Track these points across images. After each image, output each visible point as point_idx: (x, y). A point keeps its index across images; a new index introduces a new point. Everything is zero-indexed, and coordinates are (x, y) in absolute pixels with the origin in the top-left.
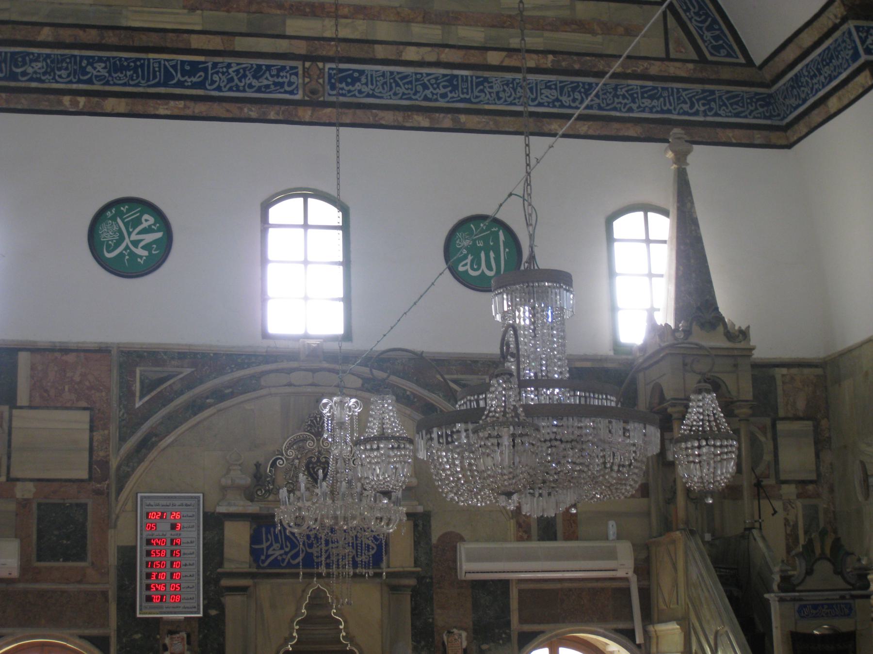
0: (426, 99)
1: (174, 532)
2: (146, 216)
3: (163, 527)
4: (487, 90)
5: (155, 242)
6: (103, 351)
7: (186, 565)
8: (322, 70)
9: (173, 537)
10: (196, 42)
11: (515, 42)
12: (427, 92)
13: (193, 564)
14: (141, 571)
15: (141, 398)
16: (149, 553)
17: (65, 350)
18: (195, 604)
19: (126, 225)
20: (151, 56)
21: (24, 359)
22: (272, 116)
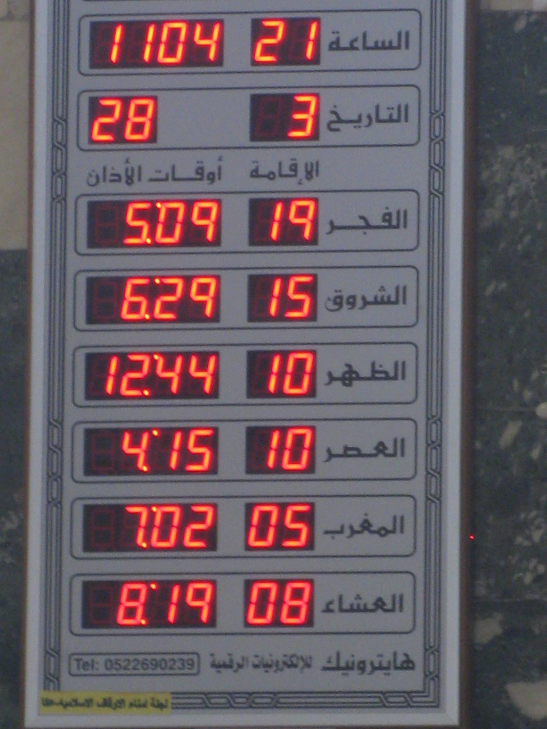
1: (271, 156)
3: (202, 118)
7: (350, 377)
9: (263, 188)
13: (398, 372)
14: (54, 423)
16: (104, 298)
18: (413, 646)
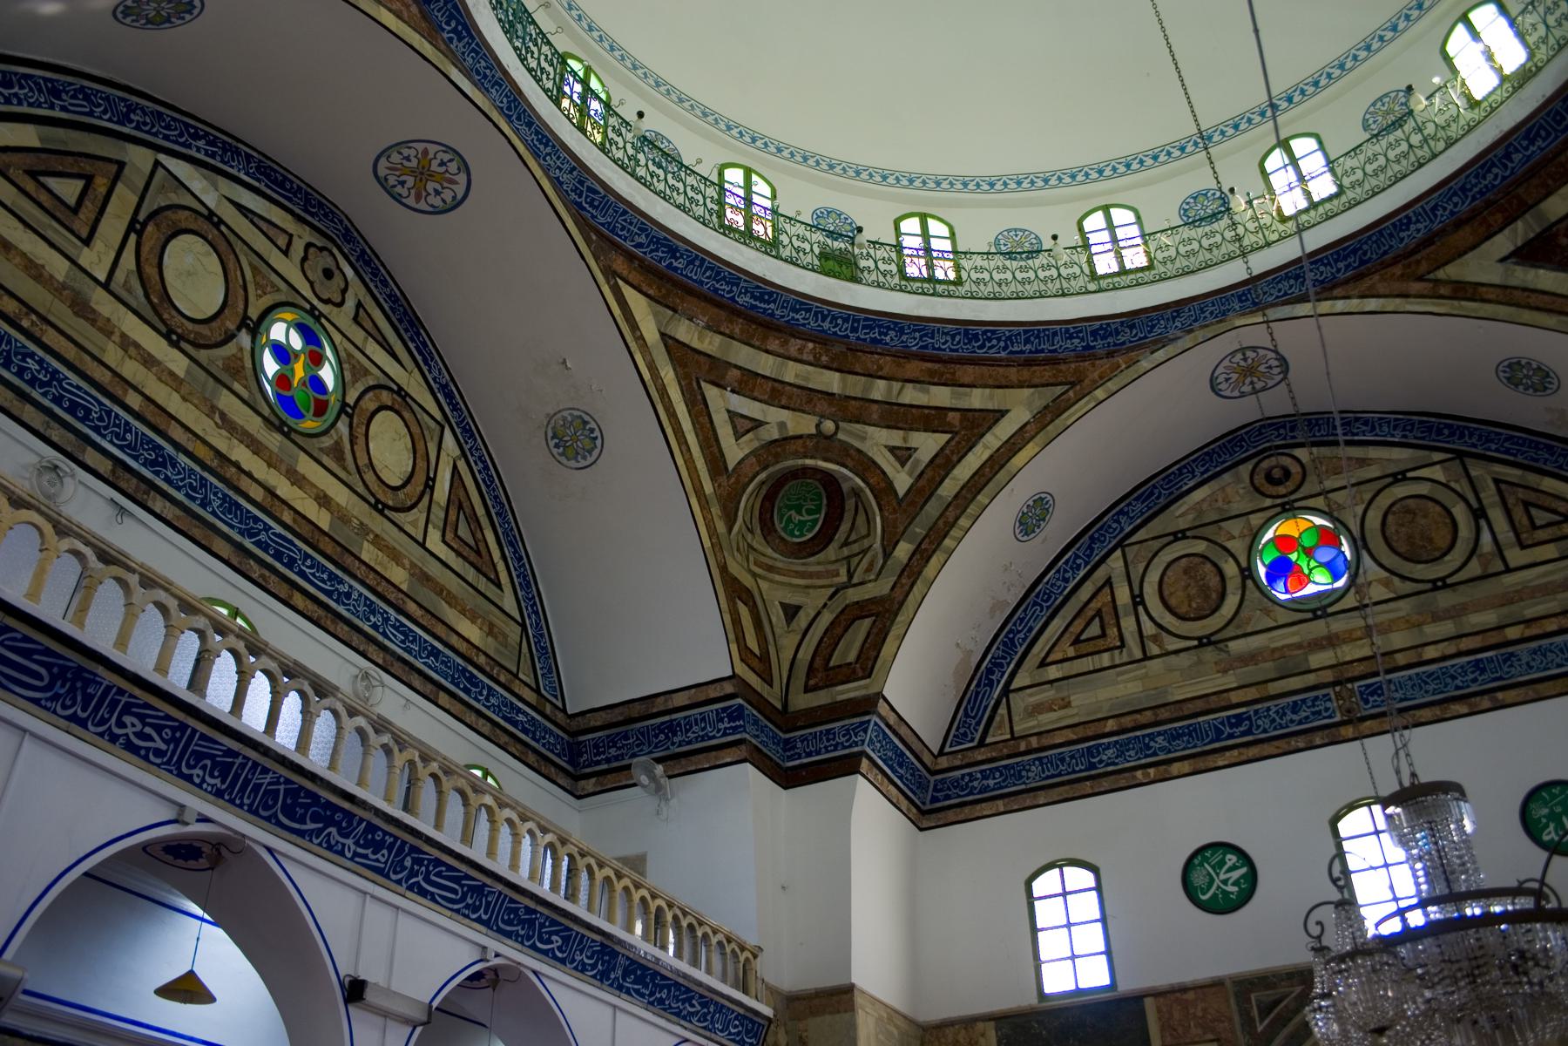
0: (1457, 688)
2: (1229, 856)
4: (1516, 664)
5: (1242, 876)
6: (1217, 984)
8: (1352, 691)
10: (1235, 697)
11: (1530, 613)
12: (1458, 682)
15: (1262, 1021)
17: (1183, 989)
19: (1213, 867)
20: (1201, 719)
21: (1148, 1002)
22: (1318, 742)
